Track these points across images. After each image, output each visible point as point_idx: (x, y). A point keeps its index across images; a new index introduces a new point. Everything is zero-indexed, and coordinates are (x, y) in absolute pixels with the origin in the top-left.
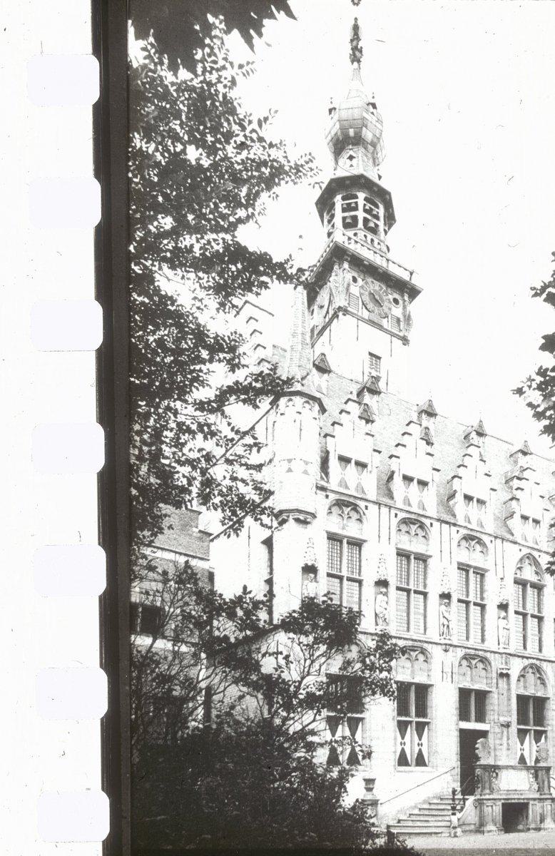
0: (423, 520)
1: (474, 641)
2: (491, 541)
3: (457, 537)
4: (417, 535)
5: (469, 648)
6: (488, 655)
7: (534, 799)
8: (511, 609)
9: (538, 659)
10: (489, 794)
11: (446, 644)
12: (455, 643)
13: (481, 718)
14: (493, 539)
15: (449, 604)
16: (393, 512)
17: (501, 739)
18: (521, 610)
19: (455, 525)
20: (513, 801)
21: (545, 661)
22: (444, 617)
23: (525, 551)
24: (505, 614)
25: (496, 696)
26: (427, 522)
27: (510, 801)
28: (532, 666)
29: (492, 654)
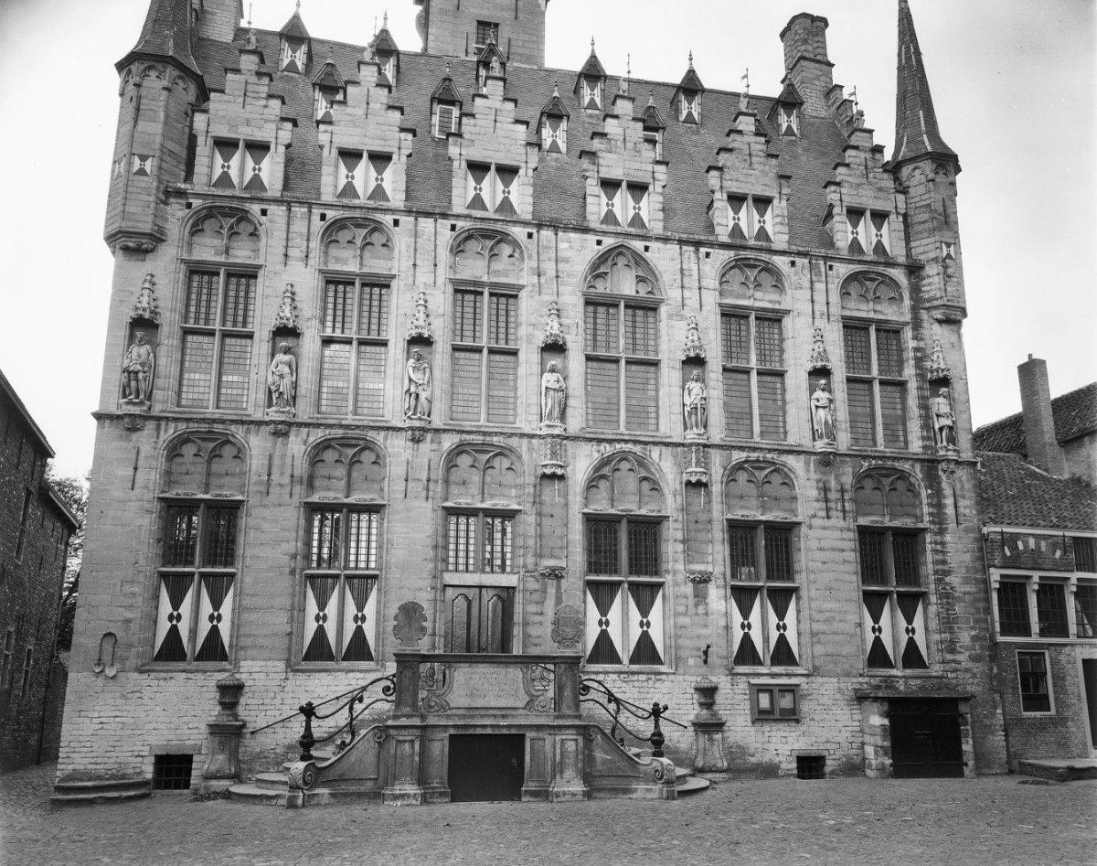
0: (379, 216)
2: (530, 236)
5: (463, 432)
6: (514, 442)
7: (539, 728)
9: (635, 442)
10: (408, 716)
11: (412, 429)
16: (316, 212)
17: (541, 603)
19: (444, 216)
20: (479, 731)
21: (654, 443)
22: (410, 380)
26: (388, 219)
27: (471, 732)
29: (525, 441)
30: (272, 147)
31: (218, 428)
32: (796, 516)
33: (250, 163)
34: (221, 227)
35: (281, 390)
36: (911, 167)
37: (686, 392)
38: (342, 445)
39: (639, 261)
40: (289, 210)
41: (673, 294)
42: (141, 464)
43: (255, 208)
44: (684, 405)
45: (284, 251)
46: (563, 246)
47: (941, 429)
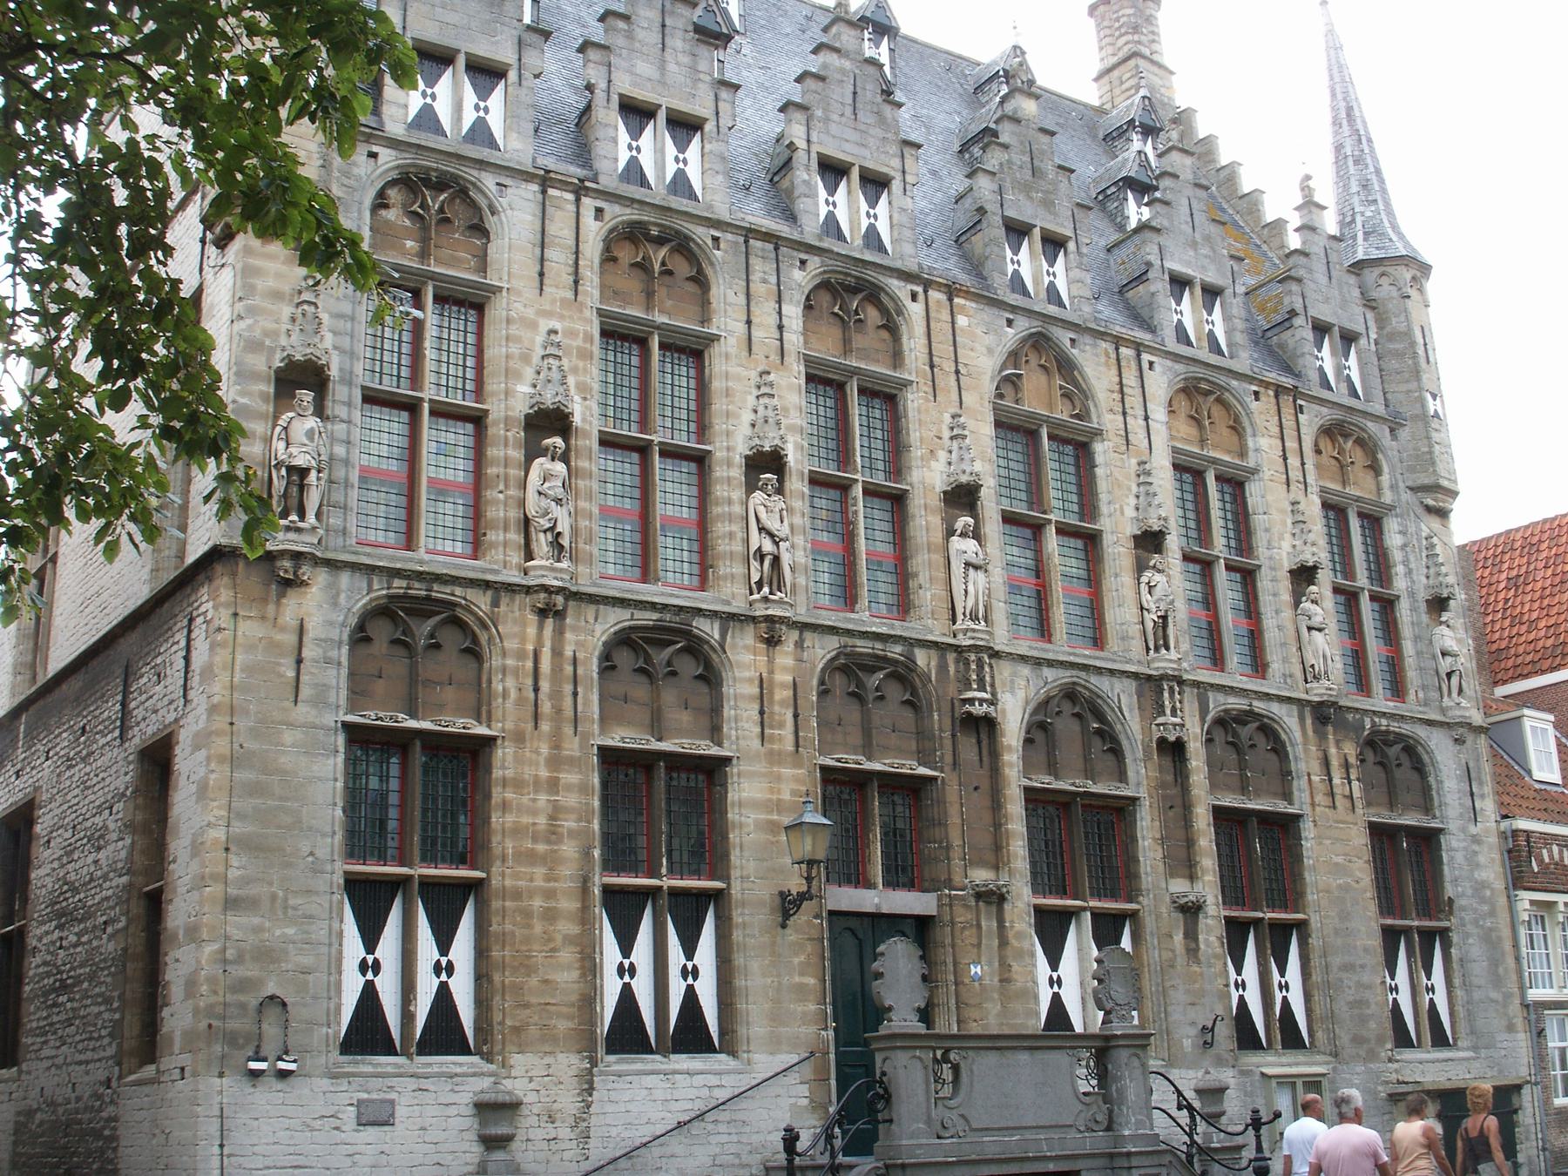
1: (866, 617)
2: (914, 297)
3: (801, 279)
4: (670, 273)
8: (990, 504)
11: (770, 619)
12: (802, 613)
13: (901, 874)
14: (919, 289)
15: (780, 491)
16: (586, 201)
18: (1021, 509)
22: (762, 529)
23: (1023, 325)
24: (970, 521)
25: (952, 793)
26: (702, 234)
28: (1070, 694)
30: (512, 75)
31: (441, 592)
32: (1291, 803)
33: (470, 96)
34: (423, 206)
35: (559, 529)
36: (1377, 271)
37: (1144, 589)
38: (648, 641)
39: (1066, 367)
40: (544, 192)
41: (1109, 421)
42: (306, 653)
43: (489, 181)
44: (1142, 608)
45: (538, 268)
46: (962, 321)
47: (1449, 675)
